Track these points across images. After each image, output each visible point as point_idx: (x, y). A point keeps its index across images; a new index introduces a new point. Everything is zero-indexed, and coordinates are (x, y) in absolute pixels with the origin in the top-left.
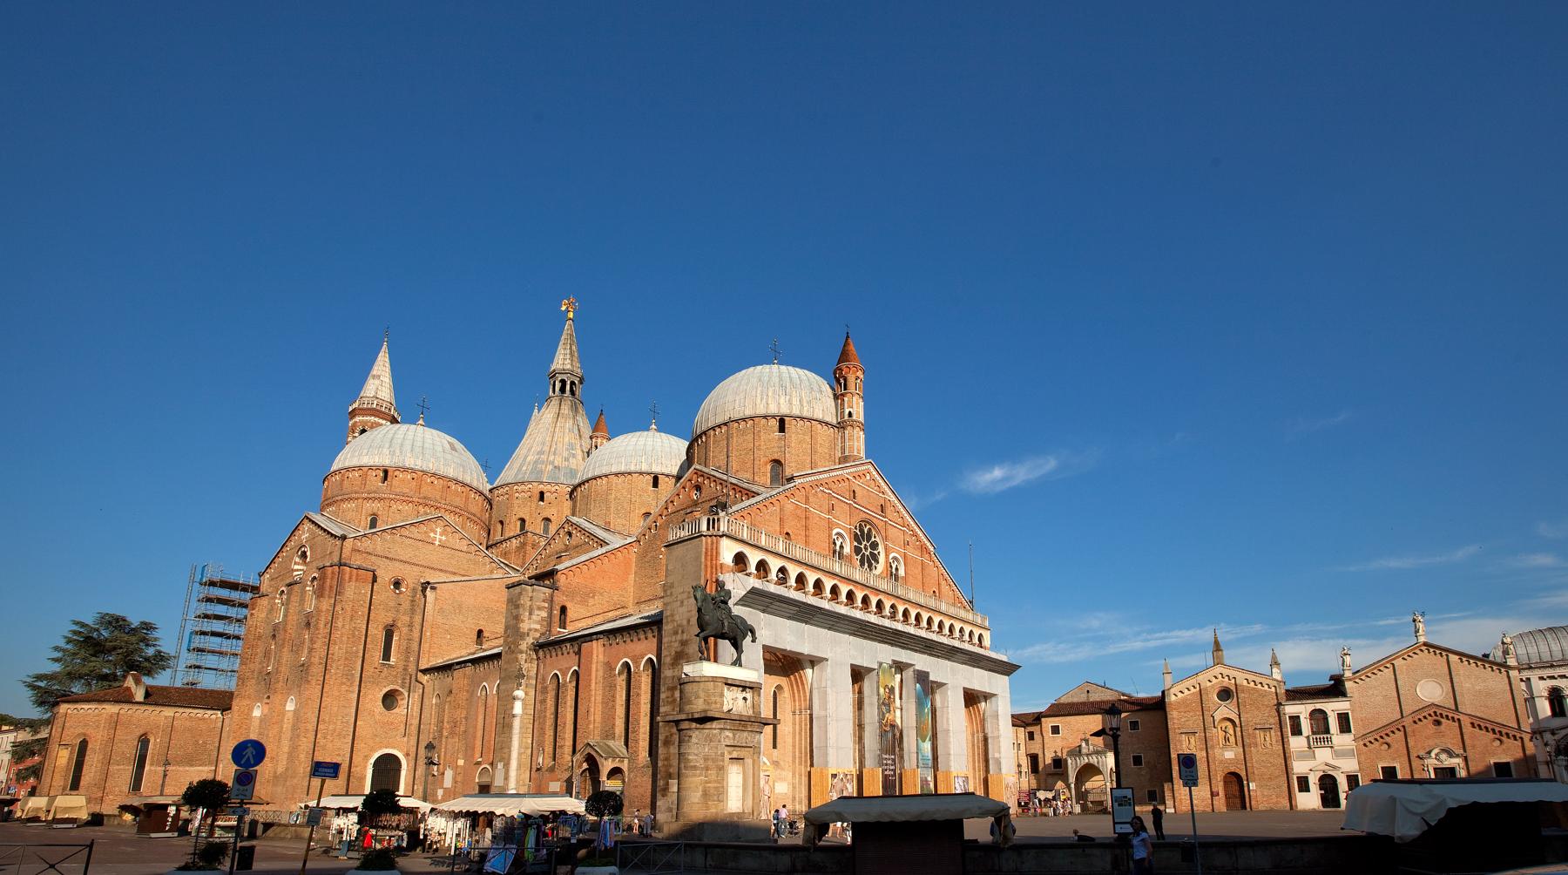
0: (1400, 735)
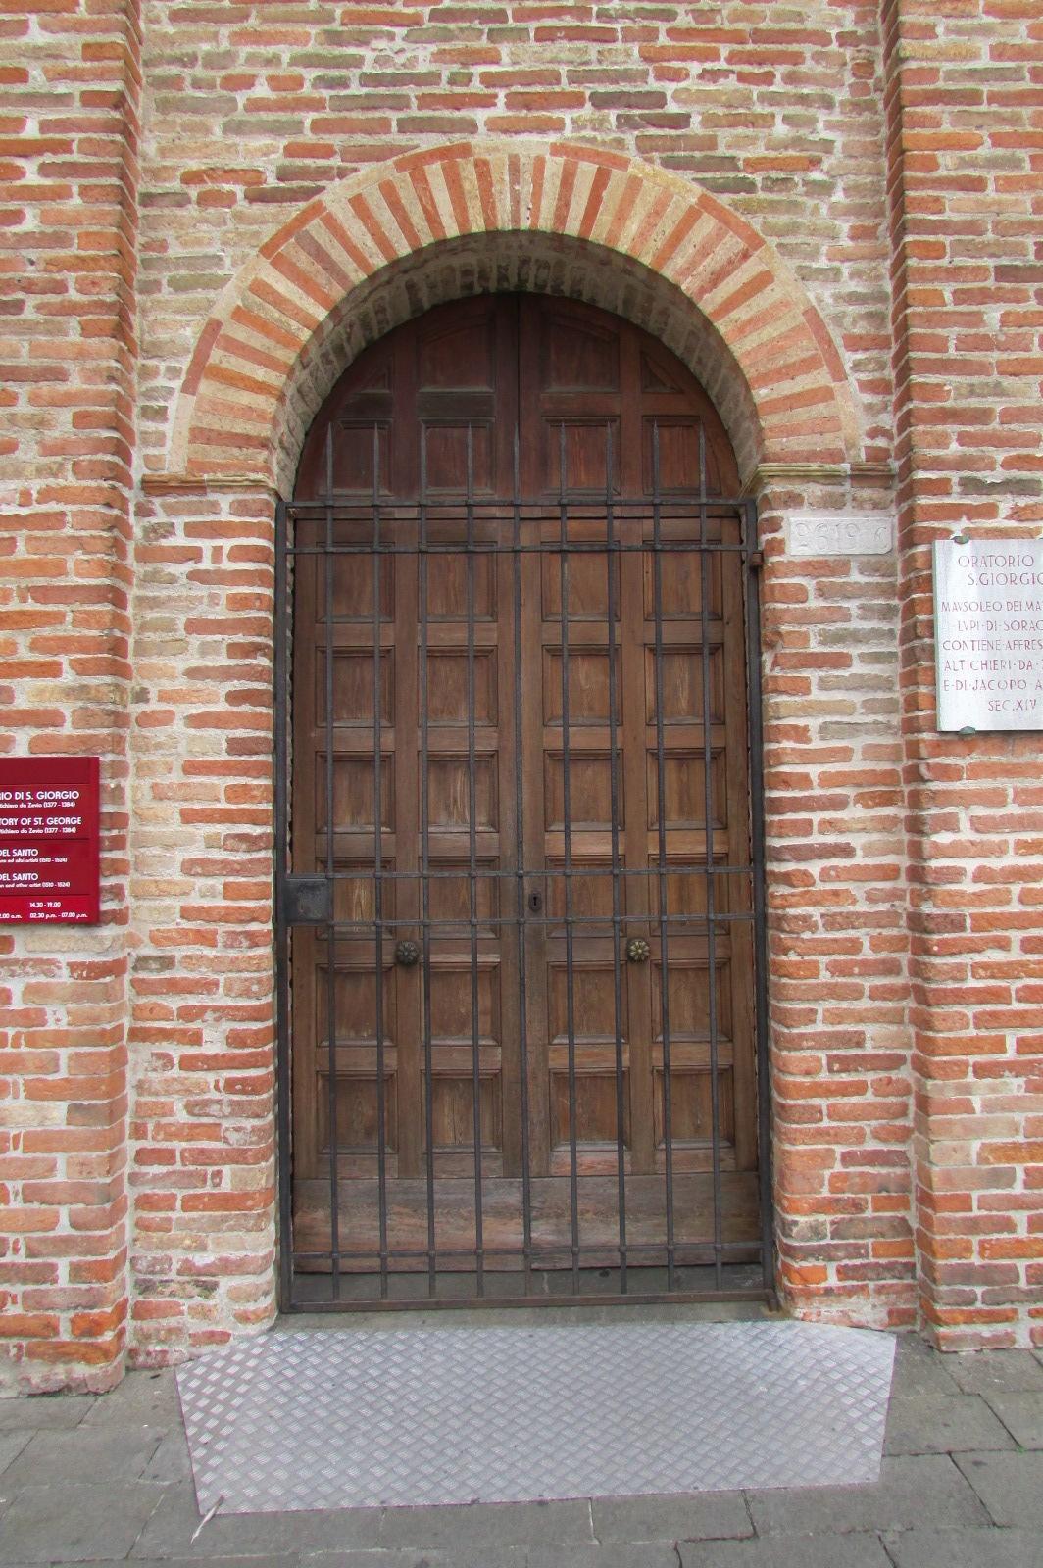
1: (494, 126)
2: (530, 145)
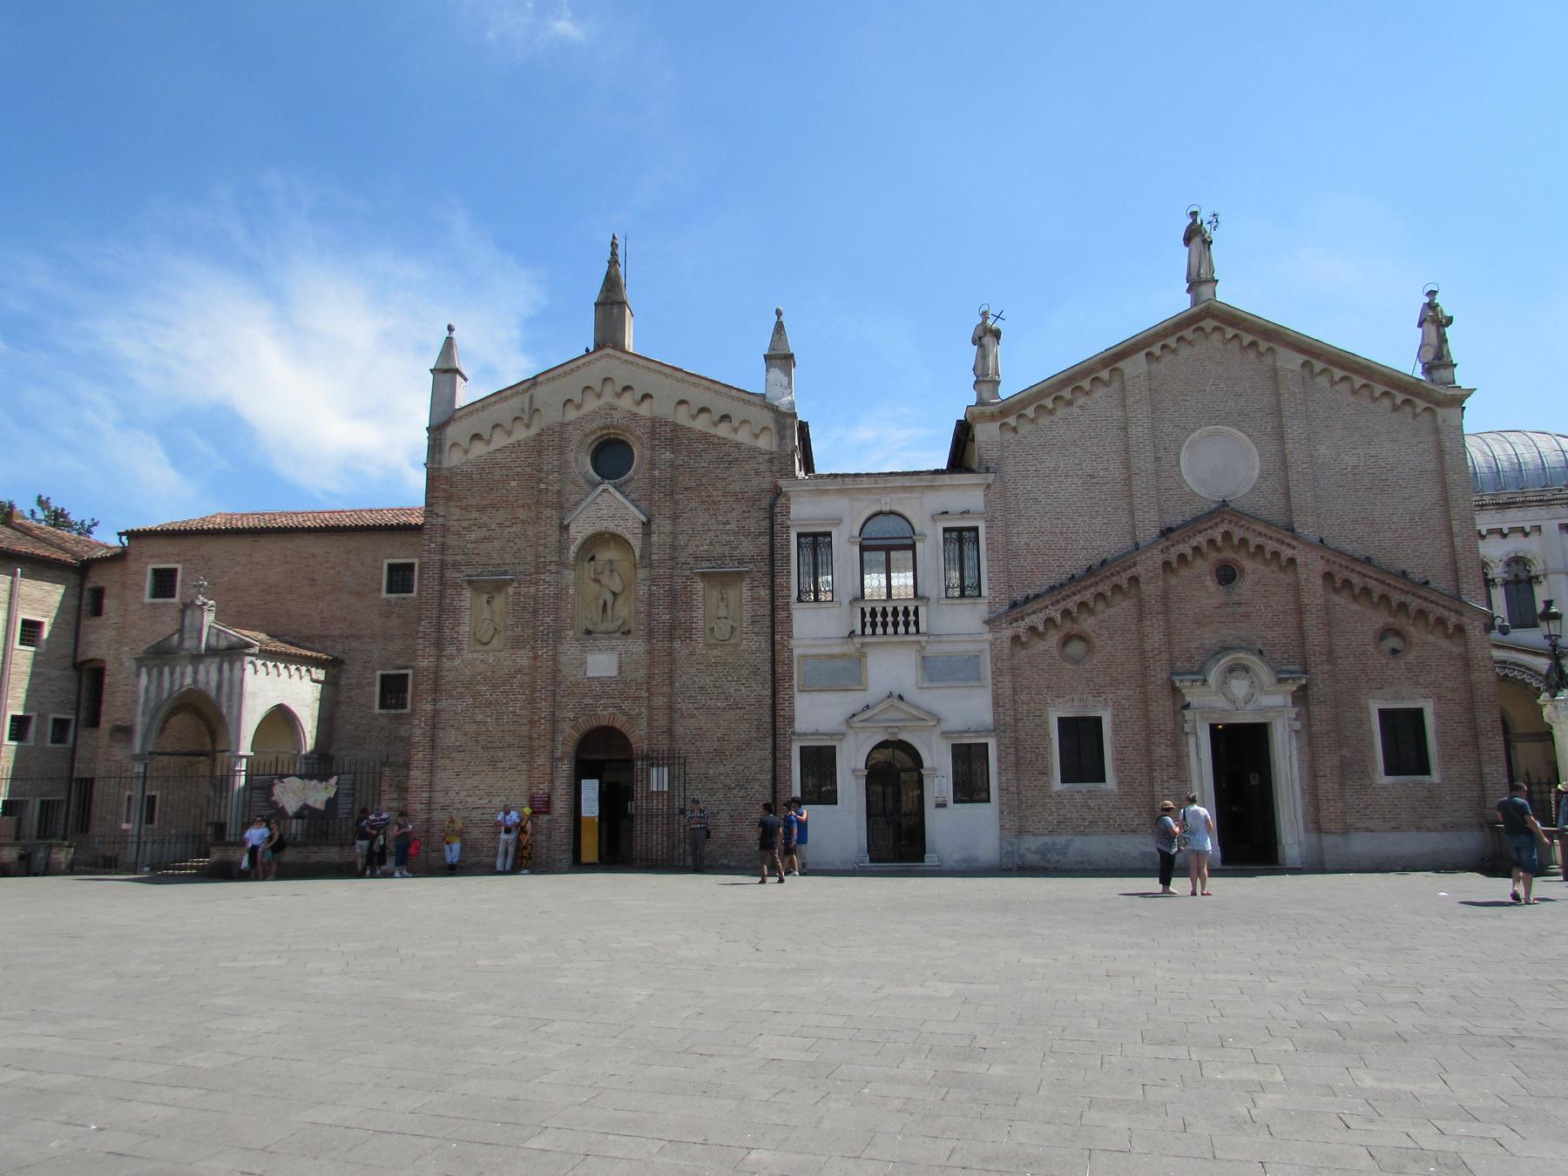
2: (605, 713)
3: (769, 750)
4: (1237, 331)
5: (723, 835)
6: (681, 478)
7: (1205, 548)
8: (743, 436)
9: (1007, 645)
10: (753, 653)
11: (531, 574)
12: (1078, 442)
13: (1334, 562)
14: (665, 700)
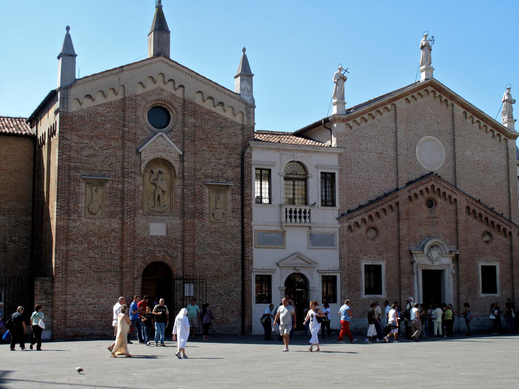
0: (391, 215)
1: (157, 253)
3: (240, 276)
4: (440, 94)
5: (218, 318)
6: (197, 133)
7: (424, 191)
8: (228, 114)
9: (346, 229)
10: (233, 227)
11: (119, 177)
12: (376, 137)
13: (470, 202)
14: (192, 249)
